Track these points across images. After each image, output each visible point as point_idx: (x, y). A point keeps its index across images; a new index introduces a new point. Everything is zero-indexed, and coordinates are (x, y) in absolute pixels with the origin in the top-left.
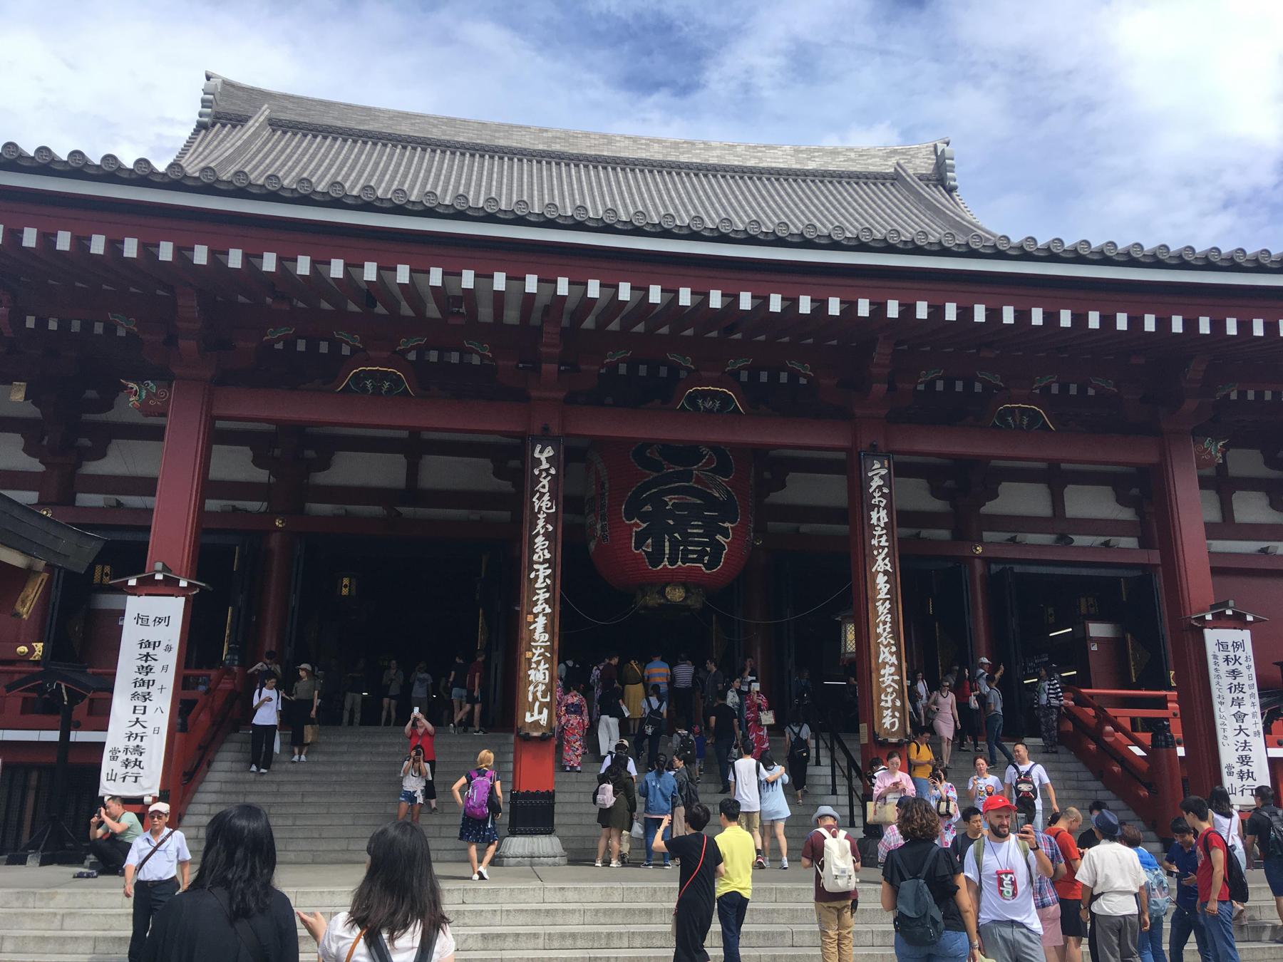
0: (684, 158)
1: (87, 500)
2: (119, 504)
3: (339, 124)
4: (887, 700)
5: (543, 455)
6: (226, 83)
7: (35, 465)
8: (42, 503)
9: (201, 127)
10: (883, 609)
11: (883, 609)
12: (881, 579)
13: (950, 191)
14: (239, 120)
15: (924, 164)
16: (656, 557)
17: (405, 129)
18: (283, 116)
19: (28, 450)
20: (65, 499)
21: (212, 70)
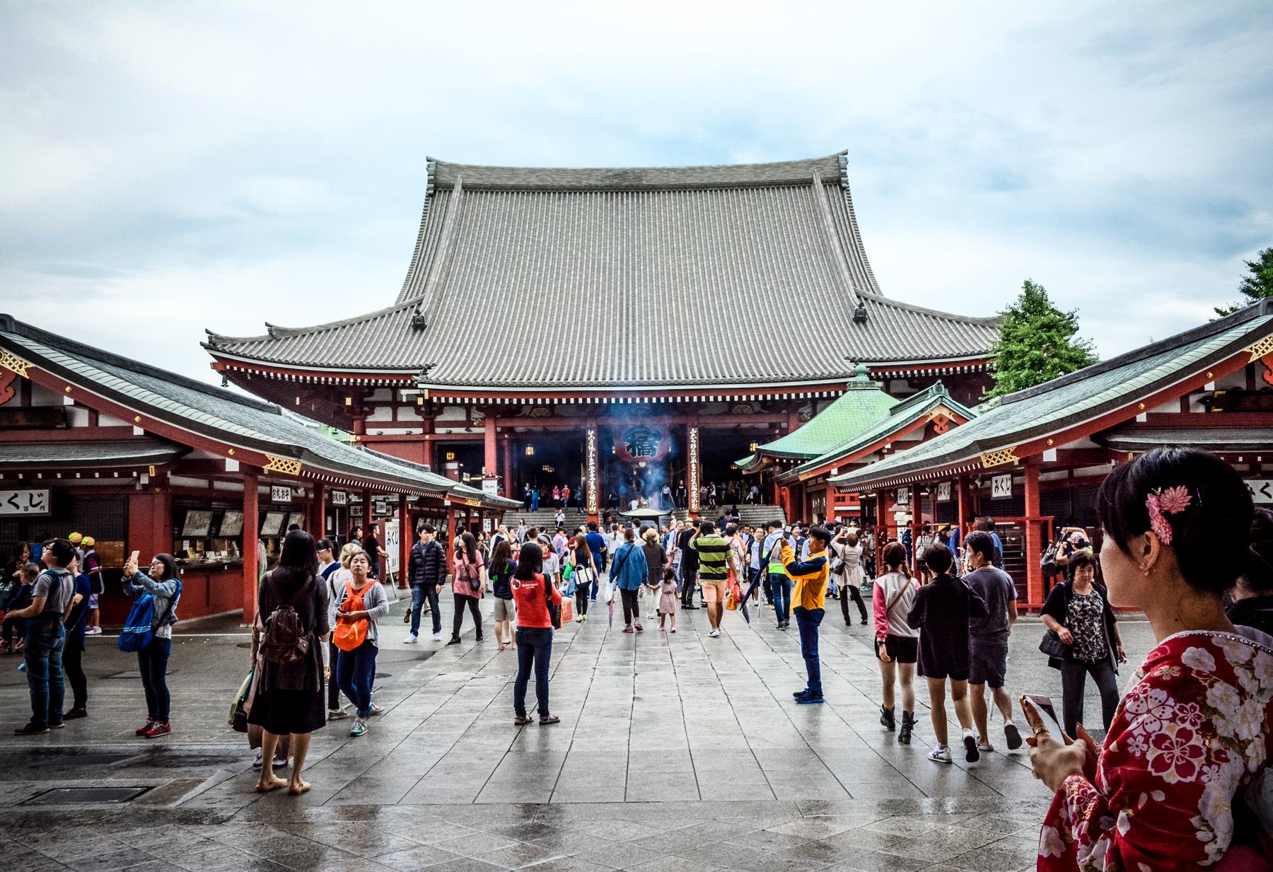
0: (689, 181)
1: (439, 431)
2: (450, 433)
3: (498, 182)
4: (693, 501)
5: (591, 433)
6: (438, 163)
7: (420, 419)
8: (425, 433)
9: (429, 196)
10: (693, 474)
11: (693, 474)
12: (694, 467)
13: (843, 189)
14: (449, 188)
15: (830, 173)
16: (634, 454)
17: (534, 181)
18: (470, 181)
19: (418, 412)
20: (432, 432)
21: (432, 156)
